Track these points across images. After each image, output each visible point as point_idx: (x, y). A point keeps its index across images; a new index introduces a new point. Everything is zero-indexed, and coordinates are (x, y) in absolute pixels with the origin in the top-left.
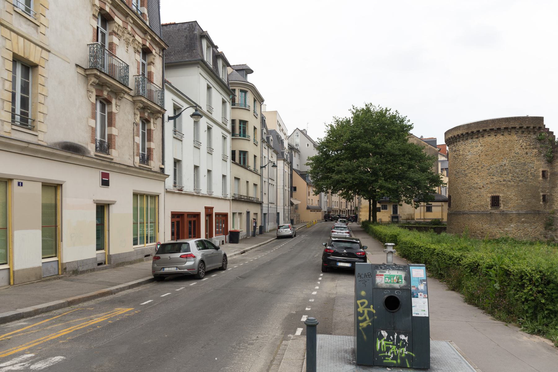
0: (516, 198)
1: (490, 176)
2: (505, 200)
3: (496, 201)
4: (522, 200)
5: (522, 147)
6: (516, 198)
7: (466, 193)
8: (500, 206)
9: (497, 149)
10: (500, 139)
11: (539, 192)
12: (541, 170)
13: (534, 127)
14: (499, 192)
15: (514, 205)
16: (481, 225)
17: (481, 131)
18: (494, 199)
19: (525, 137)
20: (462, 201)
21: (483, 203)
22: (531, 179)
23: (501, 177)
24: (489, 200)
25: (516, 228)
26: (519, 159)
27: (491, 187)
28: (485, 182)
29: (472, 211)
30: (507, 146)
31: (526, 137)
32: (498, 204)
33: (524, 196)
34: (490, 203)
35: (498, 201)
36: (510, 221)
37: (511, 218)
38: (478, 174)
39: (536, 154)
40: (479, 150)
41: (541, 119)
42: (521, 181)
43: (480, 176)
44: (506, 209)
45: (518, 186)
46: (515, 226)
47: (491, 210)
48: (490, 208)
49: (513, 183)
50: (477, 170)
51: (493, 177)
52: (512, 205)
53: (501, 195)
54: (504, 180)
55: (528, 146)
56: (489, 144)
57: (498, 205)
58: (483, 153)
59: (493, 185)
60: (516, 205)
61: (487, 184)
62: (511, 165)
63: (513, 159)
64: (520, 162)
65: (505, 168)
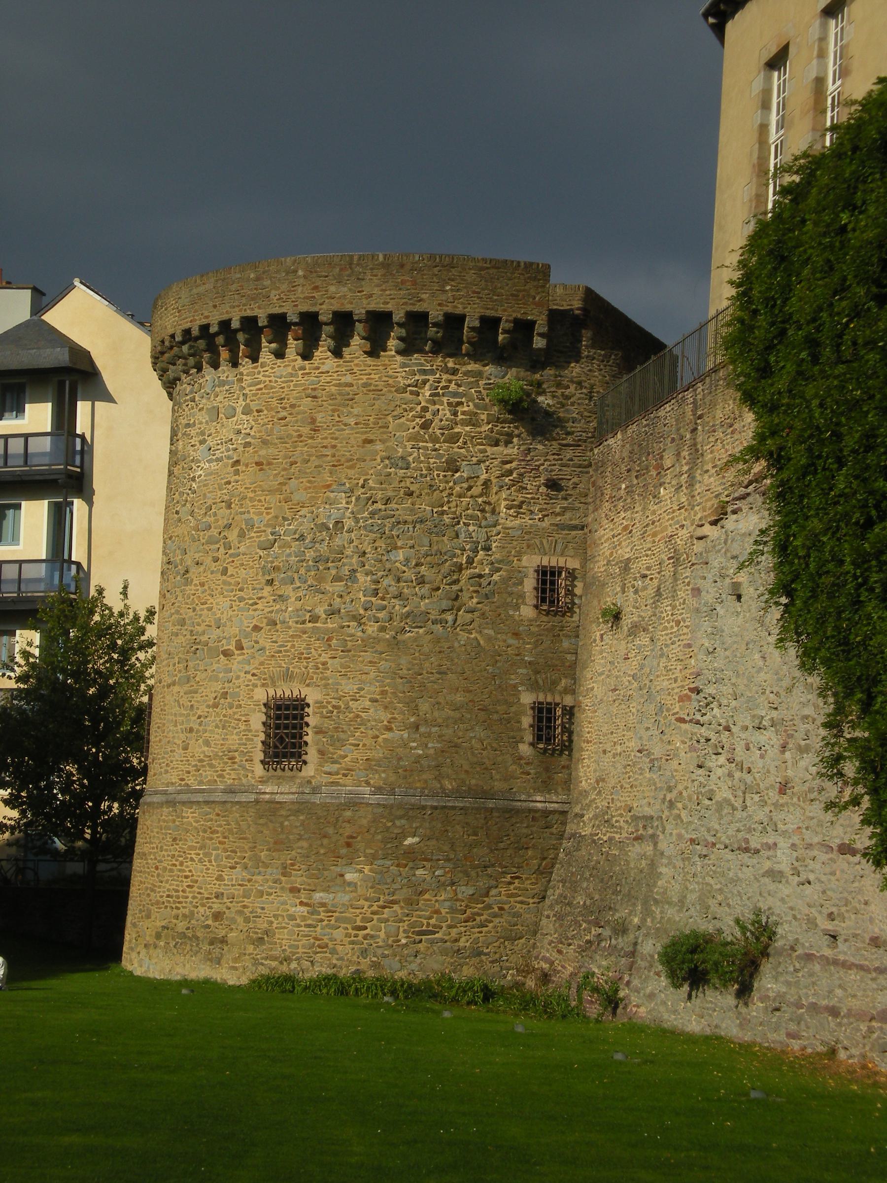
0: (385, 716)
1: (270, 582)
5: (425, 426)
6: (385, 716)
9: (305, 430)
10: (324, 378)
11: (515, 687)
12: (531, 562)
15: (370, 754)
17: (235, 324)
19: (447, 370)
21: (233, 740)
24: (257, 720)
28: (249, 619)
29: (189, 790)
30: (352, 421)
33: (424, 707)
34: (262, 737)
36: (344, 851)
37: (348, 830)
38: (225, 572)
39: (510, 472)
40: (239, 432)
42: (419, 619)
43: (233, 581)
44: (332, 779)
45: (395, 644)
48: (259, 770)
51: (288, 590)
53: (312, 696)
54: (332, 613)
55: (464, 423)
56: (274, 403)
58: (251, 449)
61: (257, 628)
65: (338, 541)
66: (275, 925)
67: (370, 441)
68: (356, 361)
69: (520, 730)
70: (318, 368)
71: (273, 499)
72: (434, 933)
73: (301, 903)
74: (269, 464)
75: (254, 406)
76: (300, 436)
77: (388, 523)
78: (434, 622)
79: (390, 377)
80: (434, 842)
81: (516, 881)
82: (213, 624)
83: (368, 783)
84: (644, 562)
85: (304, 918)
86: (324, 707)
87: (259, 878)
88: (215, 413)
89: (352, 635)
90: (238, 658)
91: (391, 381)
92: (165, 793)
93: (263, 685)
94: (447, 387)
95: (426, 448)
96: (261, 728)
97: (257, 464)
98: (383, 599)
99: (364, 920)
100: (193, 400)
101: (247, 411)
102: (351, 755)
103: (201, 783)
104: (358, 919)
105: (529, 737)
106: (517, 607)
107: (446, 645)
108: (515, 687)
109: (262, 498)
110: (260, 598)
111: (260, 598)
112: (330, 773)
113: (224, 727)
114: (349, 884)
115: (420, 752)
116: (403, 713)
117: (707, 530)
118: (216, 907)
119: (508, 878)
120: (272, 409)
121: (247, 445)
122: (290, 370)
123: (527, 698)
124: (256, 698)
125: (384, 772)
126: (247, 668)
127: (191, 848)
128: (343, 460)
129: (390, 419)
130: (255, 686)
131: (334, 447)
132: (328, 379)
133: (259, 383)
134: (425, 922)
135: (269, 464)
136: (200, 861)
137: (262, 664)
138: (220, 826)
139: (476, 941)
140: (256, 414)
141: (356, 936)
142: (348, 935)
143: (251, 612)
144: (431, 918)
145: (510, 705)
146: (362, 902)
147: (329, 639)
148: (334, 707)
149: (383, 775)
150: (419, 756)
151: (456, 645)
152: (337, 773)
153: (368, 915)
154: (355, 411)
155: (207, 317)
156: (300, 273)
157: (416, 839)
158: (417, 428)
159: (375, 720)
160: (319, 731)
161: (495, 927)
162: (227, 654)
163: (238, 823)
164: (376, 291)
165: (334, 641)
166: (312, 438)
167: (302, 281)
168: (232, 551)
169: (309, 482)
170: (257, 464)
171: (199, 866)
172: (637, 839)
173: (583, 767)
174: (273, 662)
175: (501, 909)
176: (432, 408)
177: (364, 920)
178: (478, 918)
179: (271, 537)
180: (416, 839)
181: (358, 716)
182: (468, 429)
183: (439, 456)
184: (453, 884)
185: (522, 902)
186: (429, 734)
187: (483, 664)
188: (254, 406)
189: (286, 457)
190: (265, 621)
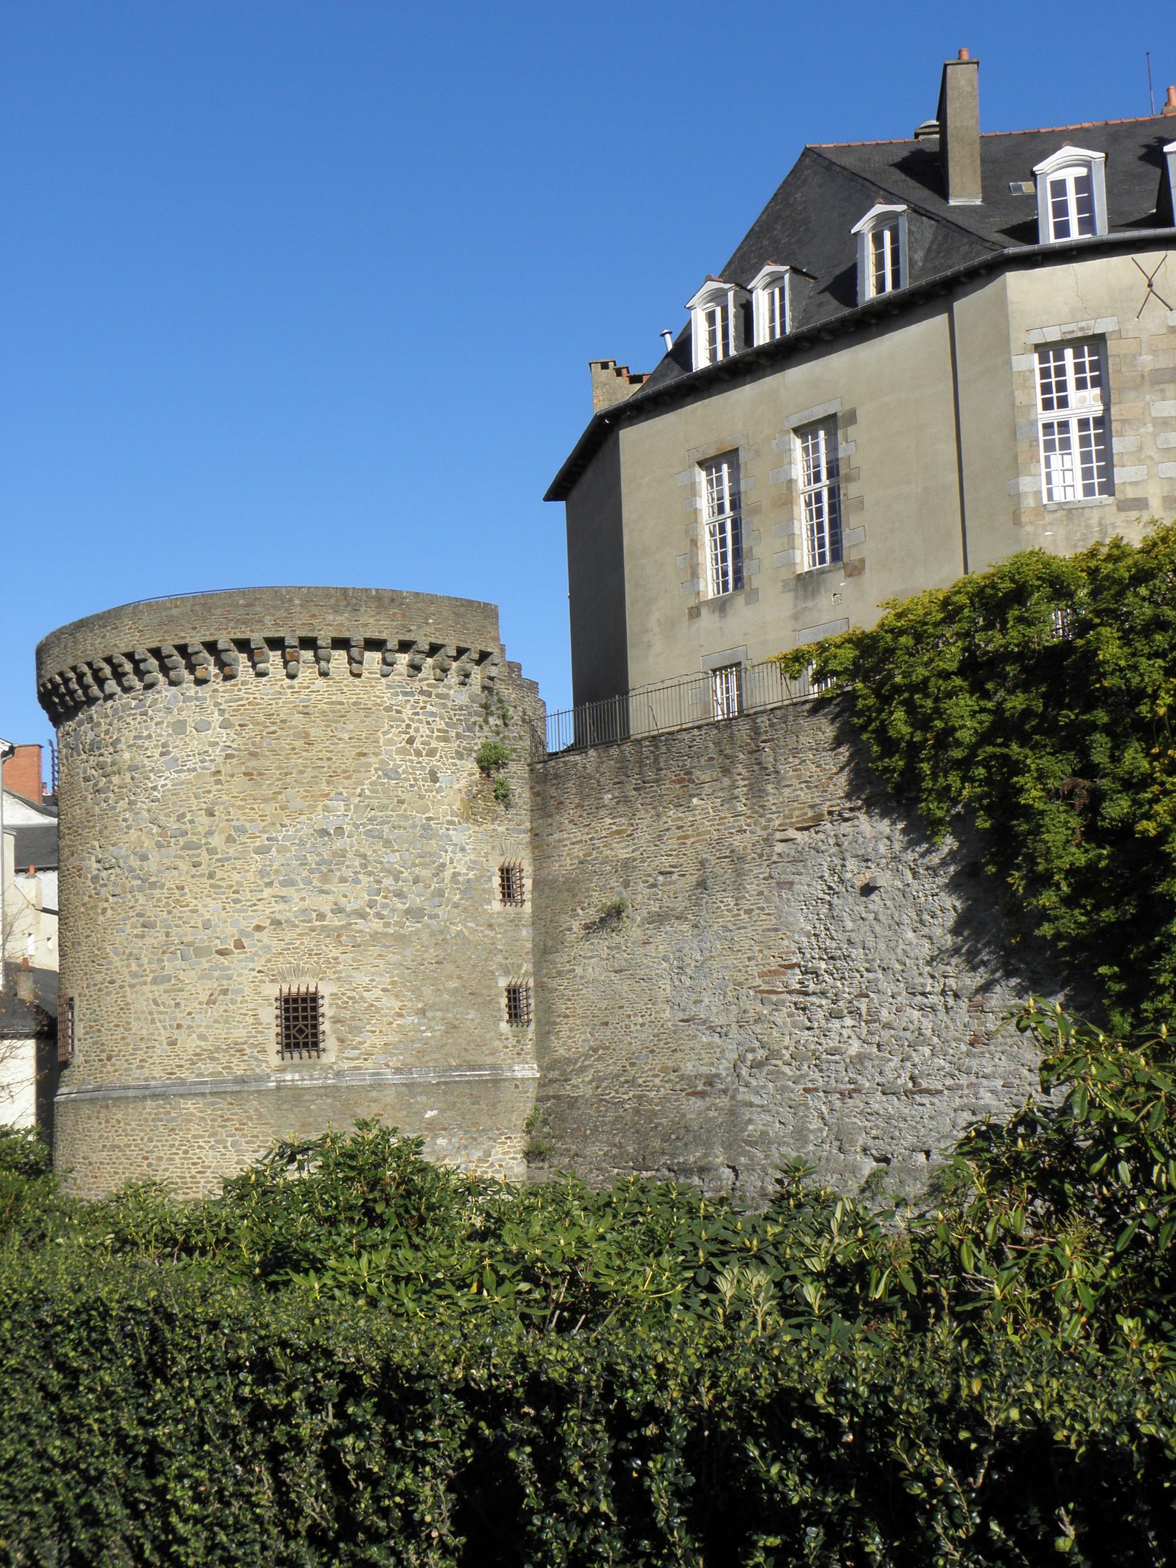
2: (348, 1014)
4: (422, 1012)
5: (411, 741)
7: (155, 981)
8: (322, 1045)
11: (493, 972)
13: (461, 652)
14: (320, 975)
15: (385, 1039)
18: (296, 1010)
19: (422, 692)
20: (135, 1026)
21: (239, 1034)
22: (456, 906)
23: (322, 892)
24: (270, 1016)
26: (401, 802)
27: (277, 946)
29: (183, 1082)
30: (346, 736)
32: (315, 1035)
33: (428, 991)
35: (315, 1018)
38: (211, 876)
43: (224, 884)
45: (401, 939)
47: (282, 1070)
48: (274, 1060)
49: (376, 925)
50: (205, 853)
52: (379, 1041)
56: (261, 718)
57: (315, 1044)
58: (235, 761)
59: (288, 935)
60: (394, 1038)
61: (258, 928)
62: (369, 833)
63: (375, 802)
65: (339, 844)
67: (364, 755)
68: (345, 682)
69: (500, 1010)
71: (270, 808)
74: (260, 774)
75: (236, 721)
76: (294, 749)
77: (386, 828)
78: (430, 917)
80: (449, 1113)
82: (200, 925)
83: (387, 1065)
86: (339, 999)
89: (361, 931)
91: (379, 701)
92: (146, 1087)
93: (272, 981)
95: (411, 761)
96: (274, 1022)
98: (385, 897)
100: (145, 714)
101: (225, 725)
102: (371, 1041)
103: (199, 1075)
105: (507, 1017)
106: (489, 902)
108: (493, 972)
109: (255, 806)
110: (259, 900)
111: (259, 900)
112: (351, 1059)
113: (226, 1022)
116: (411, 1000)
117: (791, 833)
120: (259, 724)
121: (228, 756)
122: (277, 688)
123: (503, 983)
124: (265, 993)
125: (401, 1054)
126: (251, 965)
127: (194, 1136)
128: (339, 771)
129: (380, 734)
131: (329, 759)
132: (319, 698)
133: (241, 699)
135: (260, 774)
137: (269, 961)
138: (236, 1114)
140: (238, 728)
143: (250, 913)
145: (489, 987)
147: (339, 936)
148: (350, 998)
152: (357, 1059)
154: (350, 727)
155: (184, 638)
156: (297, 602)
157: (435, 1112)
158: (404, 744)
159: (388, 1008)
160: (336, 1021)
162: (222, 953)
163: (257, 1110)
164: (371, 621)
165: (344, 938)
168: (219, 856)
169: (306, 791)
171: (211, 1153)
172: (694, 1094)
173: (558, 1039)
174: (281, 959)
175: (501, 1166)
179: (267, 843)
181: (372, 1005)
182: (442, 744)
183: (423, 768)
184: (466, 1147)
185: (513, 1158)
186: (434, 1018)
187: (469, 953)
188: (236, 721)
189: (279, 768)
190: (269, 921)
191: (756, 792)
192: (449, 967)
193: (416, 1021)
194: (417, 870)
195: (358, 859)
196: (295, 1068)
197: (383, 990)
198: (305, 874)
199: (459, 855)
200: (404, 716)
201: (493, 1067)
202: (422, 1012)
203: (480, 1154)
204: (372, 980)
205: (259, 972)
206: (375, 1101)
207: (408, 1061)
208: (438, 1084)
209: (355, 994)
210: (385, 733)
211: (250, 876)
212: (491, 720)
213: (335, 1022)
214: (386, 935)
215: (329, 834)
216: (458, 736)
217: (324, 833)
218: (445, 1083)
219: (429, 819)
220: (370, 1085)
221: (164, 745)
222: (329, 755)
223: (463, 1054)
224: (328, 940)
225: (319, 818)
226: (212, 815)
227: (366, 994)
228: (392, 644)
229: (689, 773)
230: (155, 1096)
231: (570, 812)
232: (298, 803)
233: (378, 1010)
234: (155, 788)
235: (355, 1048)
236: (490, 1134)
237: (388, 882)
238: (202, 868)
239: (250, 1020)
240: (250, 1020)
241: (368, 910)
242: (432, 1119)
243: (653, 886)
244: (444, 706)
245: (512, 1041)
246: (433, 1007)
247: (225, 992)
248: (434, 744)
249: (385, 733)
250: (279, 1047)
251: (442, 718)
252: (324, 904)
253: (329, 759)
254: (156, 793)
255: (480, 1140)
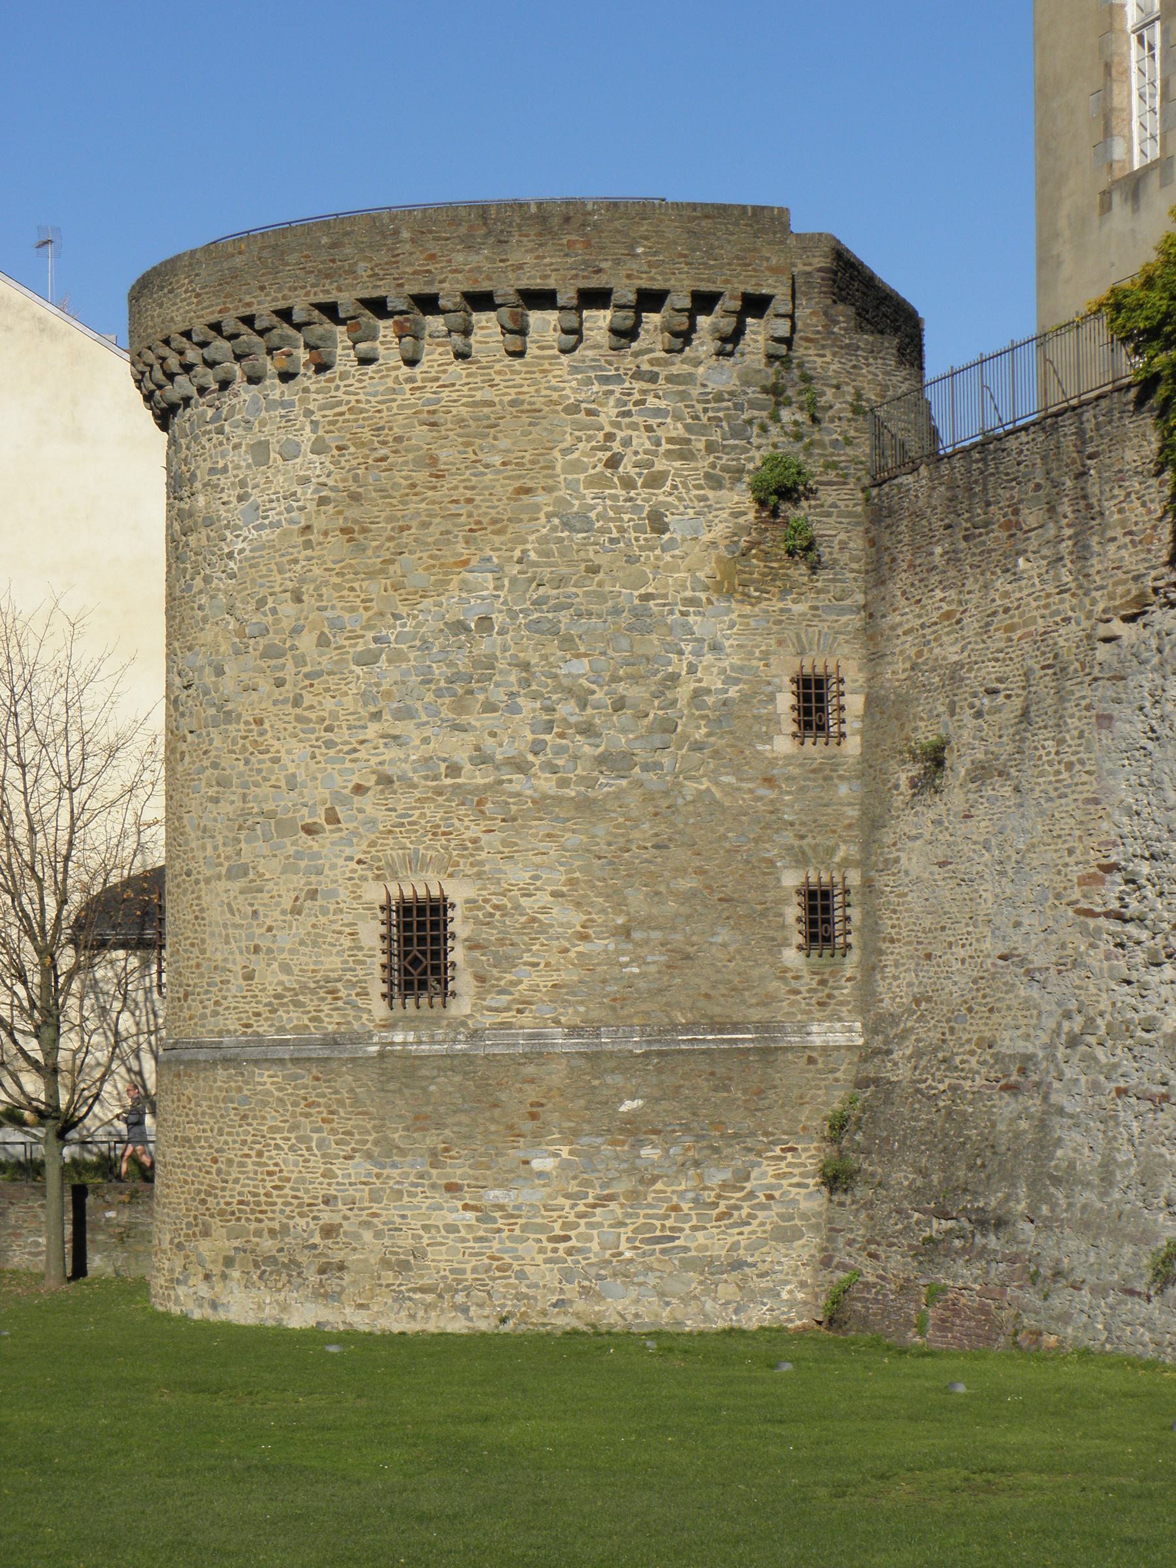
0: (577, 918)
2: (491, 935)
3: (422, 941)
4: (625, 932)
5: (613, 462)
6: (577, 918)
10: (445, 393)
11: (771, 862)
15: (556, 978)
16: (317, 1162)
19: (638, 375)
21: (332, 963)
22: (698, 747)
24: (371, 933)
25: (573, 1187)
26: (594, 570)
30: (497, 460)
31: (653, 378)
33: (637, 899)
36: (529, 1126)
37: (532, 1093)
38: (297, 702)
40: (305, 481)
41: (784, 212)
43: (313, 716)
45: (585, 806)
46: (565, 1166)
47: (389, 1026)
48: (379, 1008)
49: (546, 783)
52: (545, 981)
53: (457, 892)
56: (367, 435)
58: (330, 509)
59: (403, 801)
60: (569, 976)
61: (359, 789)
63: (546, 573)
64: (602, 597)
65: (484, 646)
66: (425, 1241)
67: (528, 491)
68: (498, 367)
69: (783, 926)
70: (437, 379)
71: (375, 588)
72: (673, 1239)
73: (466, 1207)
74: (364, 530)
75: (332, 441)
76: (413, 486)
77: (564, 617)
78: (646, 768)
79: (555, 389)
80: (665, 1105)
81: (789, 1155)
82: (283, 784)
83: (557, 1022)
84: (991, 671)
85: (469, 1227)
86: (480, 908)
87: (395, 1172)
88: (260, 451)
89: (518, 794)
90: (329, 834)
92: (218, 1046)
93: (378, 878)
94: (643, 402)
95: (615, 498)
96: (380, 945)
97: (343, 531)
98: (562, 736)
99: (565, 1226)
100: (220, 431)
101: (319, 448)
102: (528, 980)
103: (281, 1030)
104: (557, 1226)
106: (768, 739)
107: (664, 803)
108: (771, 862)
109: (356, 585)
110: (362, 742)
111: (362, 742)
112: (496, 1010)
113: (315, 944)
114: (541, 1174)
115: (636, 970)
116: (603, 911)
117: (1117, 627)
118: (326, 1217)
119: (777, 1151)
120: (363, 444)
121: (323, 501)
122: (390, 383)
123: (791, 879)
124: (367, 897)
125: (582, 1003)
126: (348, 851)
127: (273, 1129)
128: (485, 520)
129: (556, 453)
130: (364, 878)
131: (469, 501)
132: (454, 396)
133: (339, 404)
134: (658, 1223)
135: (364, 530)
136: (292, 1148)
137: (372, 844)
138: (323, 1095)
139: (735, 1247)
140: (335, 452)
141: (555, 1250)
142: (542, 1250)
143: (348, 765)
144: (667, 1217)
145: (763, 887)
146: (561, 1201)
147: (480, 803)
148: (496, 907)
149: (582, 1009)
150: (635, 976)
151: (680, 801)
152: (507, 1009)
153: (572, 1218)
154: (504, 443)
155: (249, 305)
156: (405, 235)
157: (639, 1103)
158: (600, 468)
159: (561, 925)
160: (473, 945)
161: (762, 1224)
162: (309, 830)
163: (351, 1090)
164: (529, 259)
165: (489, 805)
166: (434, 488)
167: (408, 247)
168: (307, 669)
169: (431, 557)
170: (343, 531)
171: (291, 1157)
173: (883, 979)
174: (391, 841)
175: (770, 1197)
176: (620, 435)
177: (565, 1226)
178: (736, 1213)
179: (373, 646)
180: (639, 1103)
181: (534, 920)
182: (677, 464)
183: (637, 509)
184: (697, 1164)
185: (799, 1185)
186: (647, 942)
187: (722, 829)
188: (332, 441)
189: (390, 519)
190: (374, 777)
191: (1082, 553)
192: (678, 854)
193: (612, 947)
194: (621, 688)
195: (515, 671)
196: (409, 1023)
197: (554, 894)
198: (429, 697)
199: (709, 658)
200: (603, 419)
201: (763, 1027)
202: (625, 932)
203: (727, 1175)
204: (536, 878)
205: (359, 862)
206: (532, 1081)
207: (595, 1014)
208: (646, 1055)
209: (505, 901)
210: (565, 452)
211: (348, 701)
212: (786, 415)
213: (471, 948)
214: (560, 800)
215: (468, 630)
216: (710, 448)
217: (460, 627)
218: (660, 1054)
219: (646, 597)
220: (524, 1055)
221: (243, 484)
222: (469, 494)
223: (702, 1003)
224: (463, 810)
225: (453, 605)
226: (299, 600)
227: (524, 901)
228: (566, 296)
229: (1016, 512)
230: (227, 1061)
231: (903, 578)
232: (419, 577)
233: (544, 929)
234: (230, 556)
235: (500, 992)
236: (750, 1142)
237: (567, 709)
238: (288, 690)
239: (347, 942)
240: (347, 942)
241: (530, 757)
242: (633, 1115)
243: (979, 715)
244: (683, 396)
245: (809, 981)
246: (647, 923)
247: (313, 894)
248: (660, 465)
249: (565, 452)
250: (384, 988)
251: (678, 417)
252: (459, 749)
253: (469, 501)
254: (232, 564)
255: (727, 1151)
